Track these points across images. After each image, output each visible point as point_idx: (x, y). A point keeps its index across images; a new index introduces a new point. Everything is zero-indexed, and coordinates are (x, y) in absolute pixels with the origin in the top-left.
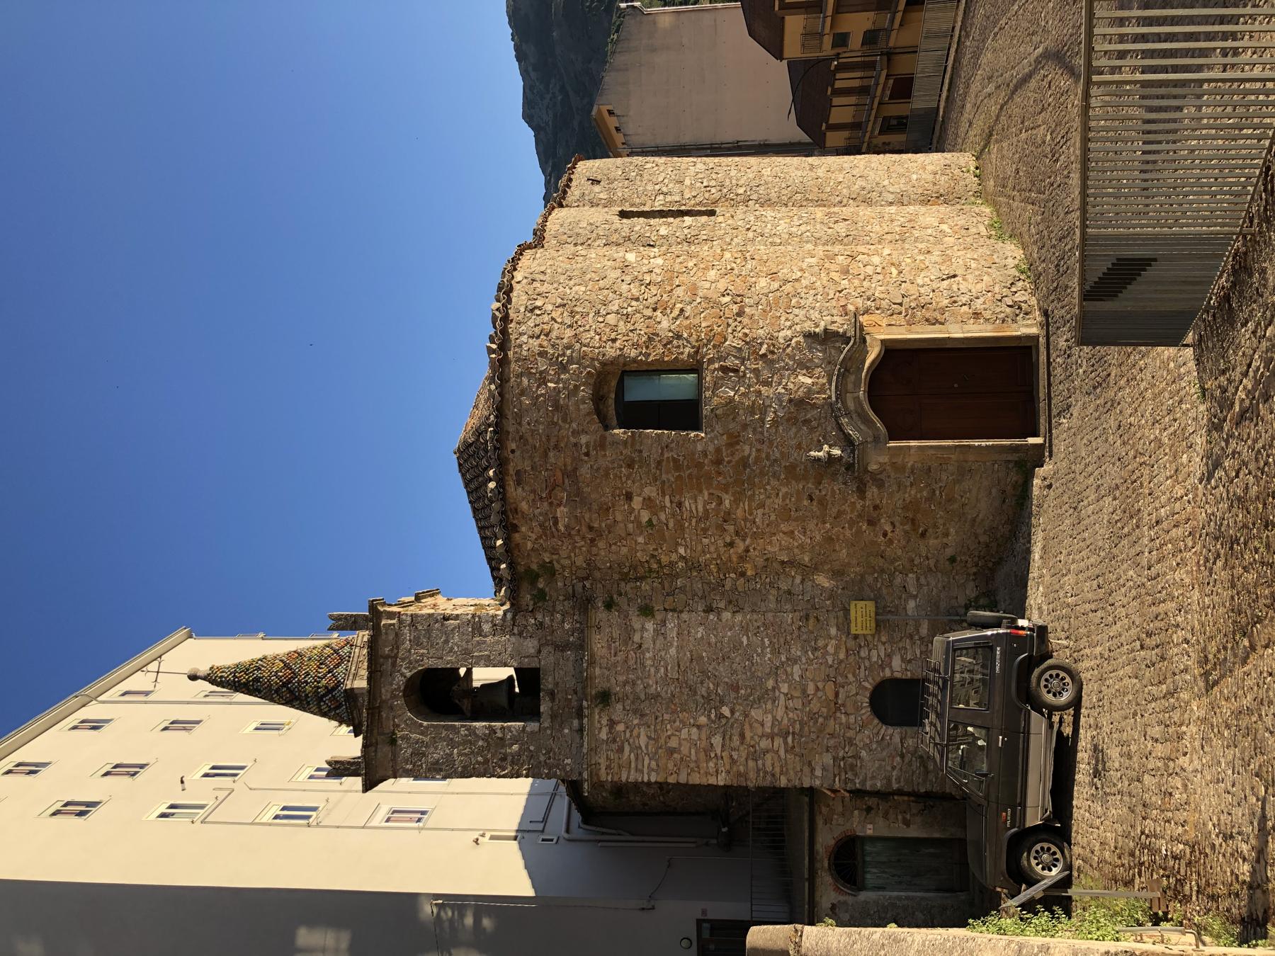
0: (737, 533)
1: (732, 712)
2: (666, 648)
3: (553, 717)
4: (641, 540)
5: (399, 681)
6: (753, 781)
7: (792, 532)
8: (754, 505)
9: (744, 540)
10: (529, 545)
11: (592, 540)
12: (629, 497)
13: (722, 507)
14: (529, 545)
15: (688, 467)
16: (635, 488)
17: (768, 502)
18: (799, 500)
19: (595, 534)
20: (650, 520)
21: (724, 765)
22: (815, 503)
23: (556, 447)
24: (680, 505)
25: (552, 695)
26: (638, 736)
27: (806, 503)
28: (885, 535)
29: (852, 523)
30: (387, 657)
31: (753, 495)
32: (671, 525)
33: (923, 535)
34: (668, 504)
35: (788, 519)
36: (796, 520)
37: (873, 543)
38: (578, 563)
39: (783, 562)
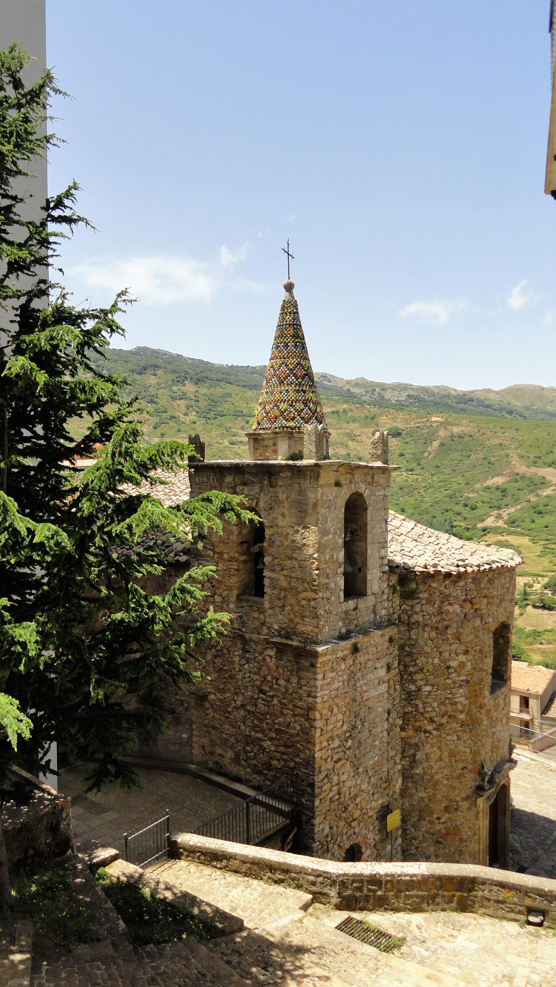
0: (441, 725)
1: (349, 748)
2: (374, 688)
3: (346, 612)
4: (436, 661)
5: (362, 488)
6: (318, 778)
7: (441, 760)
8: (460, 734)
9: (434, 729)
10: (434, 585)
11: (437, 628)
12: (466, 652)
13: (458, 713)
14: (434, 585)
15: (480, 688)
16: (470, 657)
17: (461, 742)
18: (463, 761)
19: (442, 631)
20: (452, 668)
21: (324, 754)
22: (460, 771)
23: (488, 603)
24: (460, 686)
25: (355, 609)
26: (339, 682)
27: (460, 766)
28: (438, 819)
29: (446, 797)
30: (373, 478)
31: (466, 732)
32: (448, 681)
33: (438, 842)
34: (461, 678)
35: (450, 757)
36: (450, 761)
37: (432, 813)
38: (415, 616)
39: (414, 755)
